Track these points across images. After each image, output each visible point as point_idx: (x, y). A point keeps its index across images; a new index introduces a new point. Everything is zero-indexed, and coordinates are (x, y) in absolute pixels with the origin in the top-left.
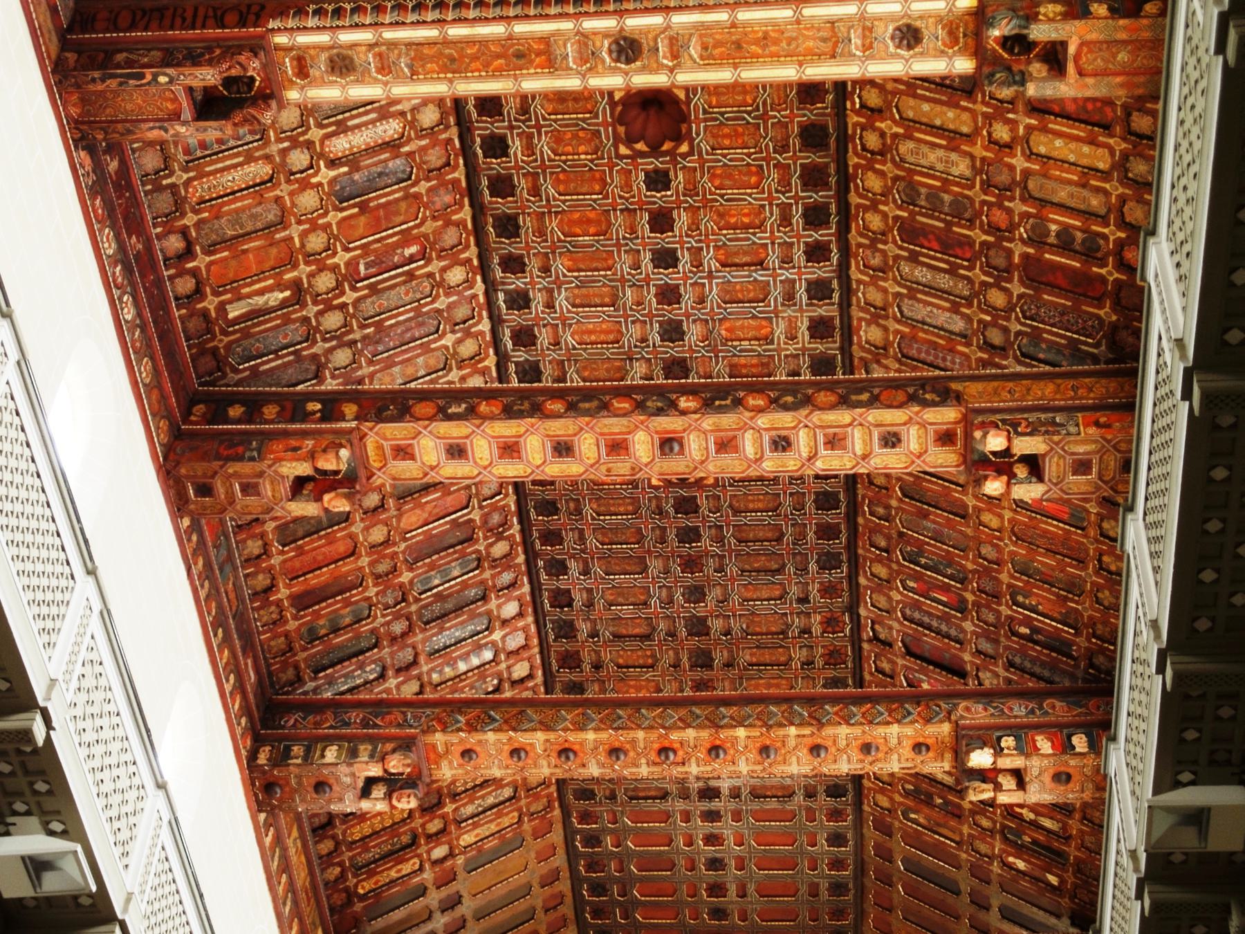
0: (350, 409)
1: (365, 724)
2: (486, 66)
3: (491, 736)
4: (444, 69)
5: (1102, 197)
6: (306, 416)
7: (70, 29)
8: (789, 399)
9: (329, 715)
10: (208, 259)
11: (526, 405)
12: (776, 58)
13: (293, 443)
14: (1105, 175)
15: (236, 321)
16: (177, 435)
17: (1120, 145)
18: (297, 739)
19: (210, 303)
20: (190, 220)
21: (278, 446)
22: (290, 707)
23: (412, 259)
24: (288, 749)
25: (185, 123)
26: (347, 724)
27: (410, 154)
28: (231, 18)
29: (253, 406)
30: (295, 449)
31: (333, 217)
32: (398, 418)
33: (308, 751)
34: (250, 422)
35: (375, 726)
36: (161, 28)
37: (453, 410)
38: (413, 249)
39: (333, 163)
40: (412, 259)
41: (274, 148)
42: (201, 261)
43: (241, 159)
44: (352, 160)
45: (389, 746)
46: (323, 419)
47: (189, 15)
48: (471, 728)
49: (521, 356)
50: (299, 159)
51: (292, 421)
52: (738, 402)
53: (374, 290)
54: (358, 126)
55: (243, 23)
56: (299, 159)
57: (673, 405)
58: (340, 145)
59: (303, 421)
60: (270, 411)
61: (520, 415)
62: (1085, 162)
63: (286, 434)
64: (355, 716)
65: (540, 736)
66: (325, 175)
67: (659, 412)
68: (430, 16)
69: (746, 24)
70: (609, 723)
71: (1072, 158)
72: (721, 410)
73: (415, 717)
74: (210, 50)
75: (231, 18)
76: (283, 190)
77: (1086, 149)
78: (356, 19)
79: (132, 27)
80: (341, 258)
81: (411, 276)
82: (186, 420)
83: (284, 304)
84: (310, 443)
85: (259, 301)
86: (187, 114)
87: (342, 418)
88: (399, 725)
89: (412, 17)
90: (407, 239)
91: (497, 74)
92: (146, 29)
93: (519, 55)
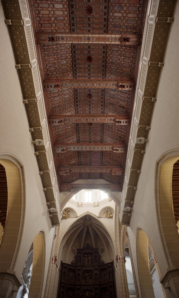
5: (40, 6)
10: (137, 5)
12: (75, 37)
14: (41, 10)
17: (40, 15)
20: (137, 12)
25: (131, 37)
27: (114, 10)
31: (123, 5)
39: (122, 13)
41: (127, 18)
43: (130, 18)
44: (120, 12)
50: (125, 15)
54: (118, 17)
56: (125, 15)
58: (120, 15)
62: (43, 11)
66: (123, 12)
71: (45, 11)
76: (127, 12)
77: (43, 13)
86: (130, 38)
91: (100, 37)
93: (98, 39)
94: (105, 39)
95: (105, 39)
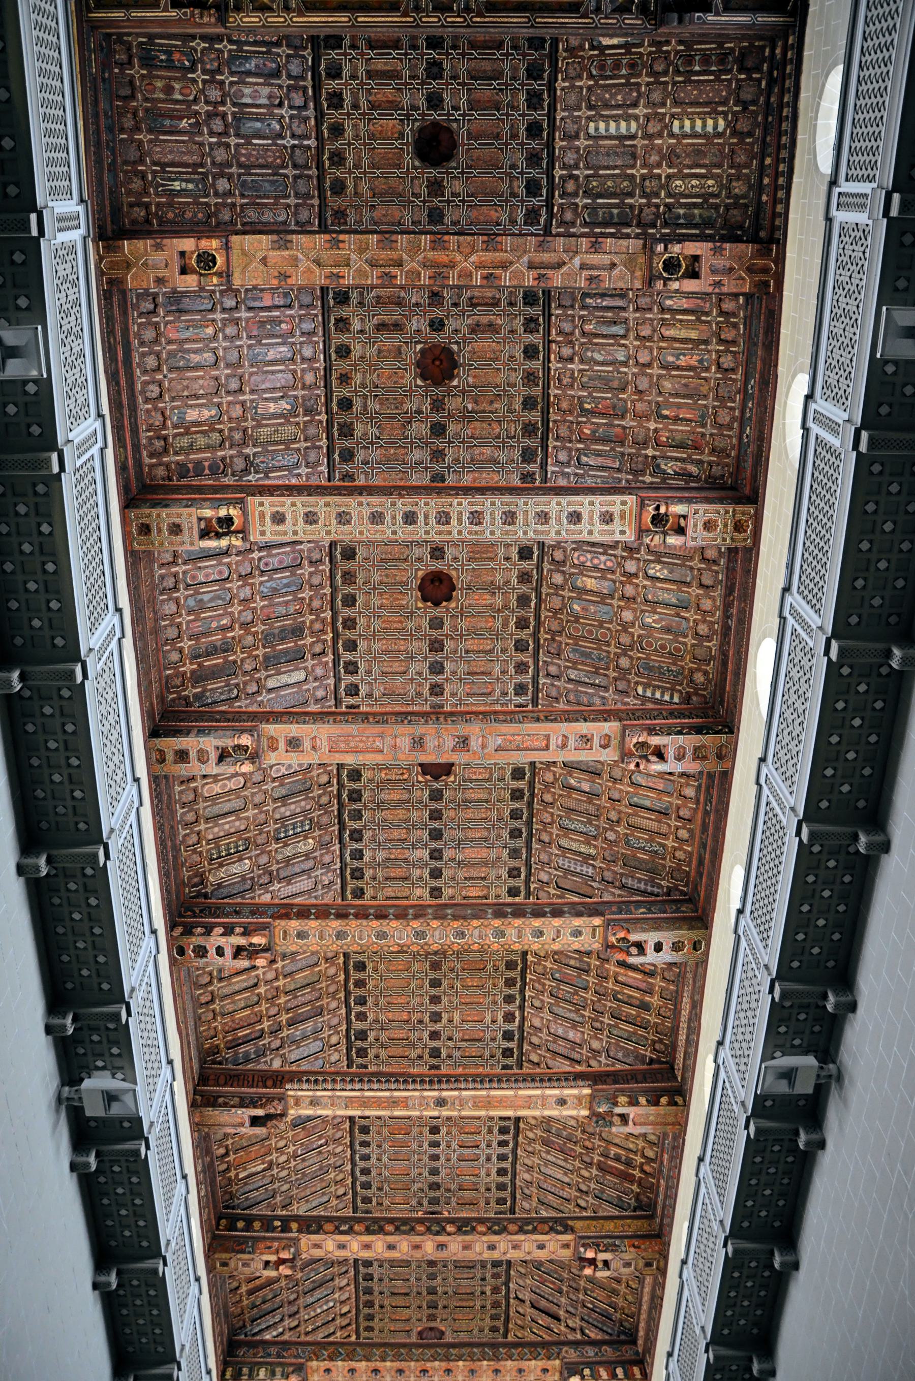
0: (294, 1226)
1: (279, 1356)
2: (379, 1106)
3: (340, 1363)
4: (361, 1106)
6: (274, 1229)
7: (198, 1085)
8: (496, 1228)
9: (260, 1349)
11: (376, 1227)
13: (269, 1244)
15: (242, 1179)
16: (214, 1237)
18: (244, 1363)
19: (232, 1174)
21: (261, 1245)
22: (240, 1344)
23: (321, 1146)
24: (241, 1369)
26: (269, 1355)
28: (269, 1083)
29: (249, 1222)
30: (270, 1248)
31: (291, 1134)
32: (316, 1232)
33: (251, 1371)
34: (247, 1231)
35: (284, 1357)
36: (238, 1086)
37: (342, 1228)
38: (322, 1141)
40: (321, 1146)
42: (232, 1157)
45: (291, 1369)
46: (282, 1231)
47: (250, 1079)
48: (331, 1359)
49: (363, 1178)
51: (267, 1231)
52: (473, 1229)
53: (303, 1160)
55: (274, 1086)
57: (444, 1229)
59: (273, 1232)
60: (257, 1225)
61: (373, 1233)
63: (264, 1238)
64: (273, 1350)
65: (364, 1363)
67: (438, 1233)
68: (358, 1086)
69: (493, 1097)
70: (397, 1358)
72: (466, 1233)
73: (303, 1352)
74: (261, 1099)
75: (269, 1083)
78: (325, 1086)
79: (225, 1085)
80: (291, 1149)
81: (320, 1152)
82: (218, 1229)
83: (264, 1170)
84: (276, 1244)
85: (254, 1170)
87: (290, 1231)
88: (295, 1357)
89: (349, 1087)
90: (320, 1137)
91: (384, 1108)
92: (231, 1086)
94: (365, 1103)
95: (365, 1103)
